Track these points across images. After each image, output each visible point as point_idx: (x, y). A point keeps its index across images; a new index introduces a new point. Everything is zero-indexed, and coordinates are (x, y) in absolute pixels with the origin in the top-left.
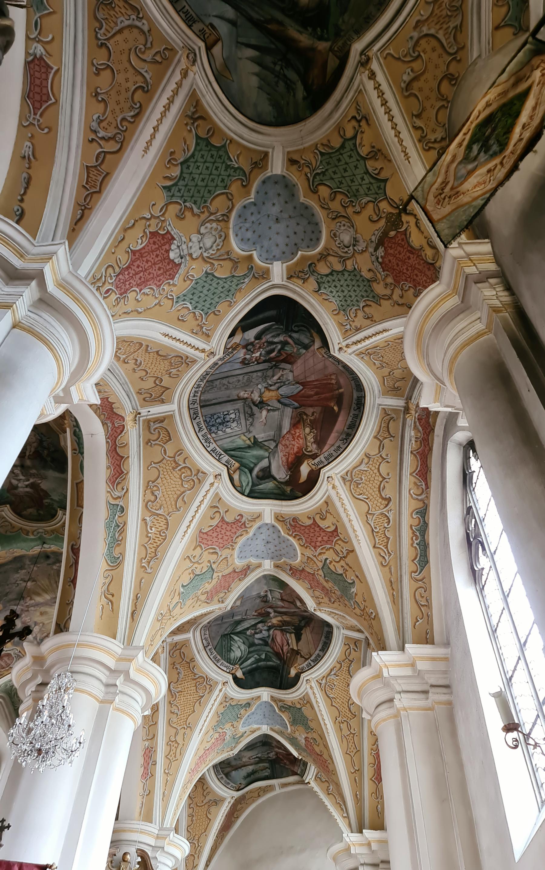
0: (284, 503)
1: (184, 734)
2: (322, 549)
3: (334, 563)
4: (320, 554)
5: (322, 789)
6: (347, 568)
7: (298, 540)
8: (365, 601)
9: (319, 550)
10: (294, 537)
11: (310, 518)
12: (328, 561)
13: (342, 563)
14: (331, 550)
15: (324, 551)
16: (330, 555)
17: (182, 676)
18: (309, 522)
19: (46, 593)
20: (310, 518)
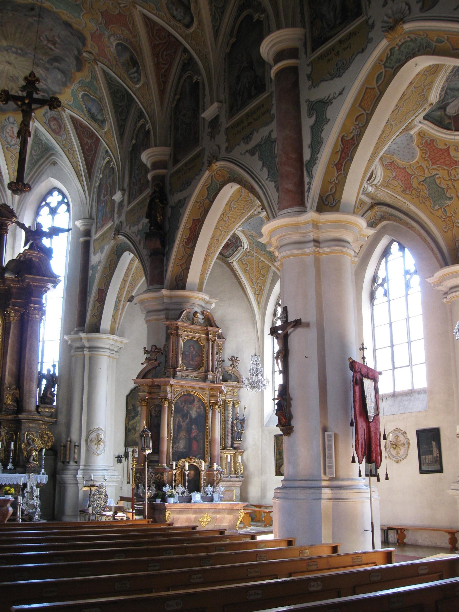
0: (436, 128)
1: (224, 236)
2: (438, 167)
3: (442, 179)
4: (434, 169)
5: (241, 268)
6: (452, 187)
7: (423, 153)
8: (455, 213)
9: (435, 167)
10: (421, 150)
11: (445, 145)
12: (437, 176)
13: (449, 182)
14: (446, 171)
15: (440, 169)
16: (442, 173)
17: (242, 197)
18: (442, 147)
19: (6, 39)
20: (445, 145)
